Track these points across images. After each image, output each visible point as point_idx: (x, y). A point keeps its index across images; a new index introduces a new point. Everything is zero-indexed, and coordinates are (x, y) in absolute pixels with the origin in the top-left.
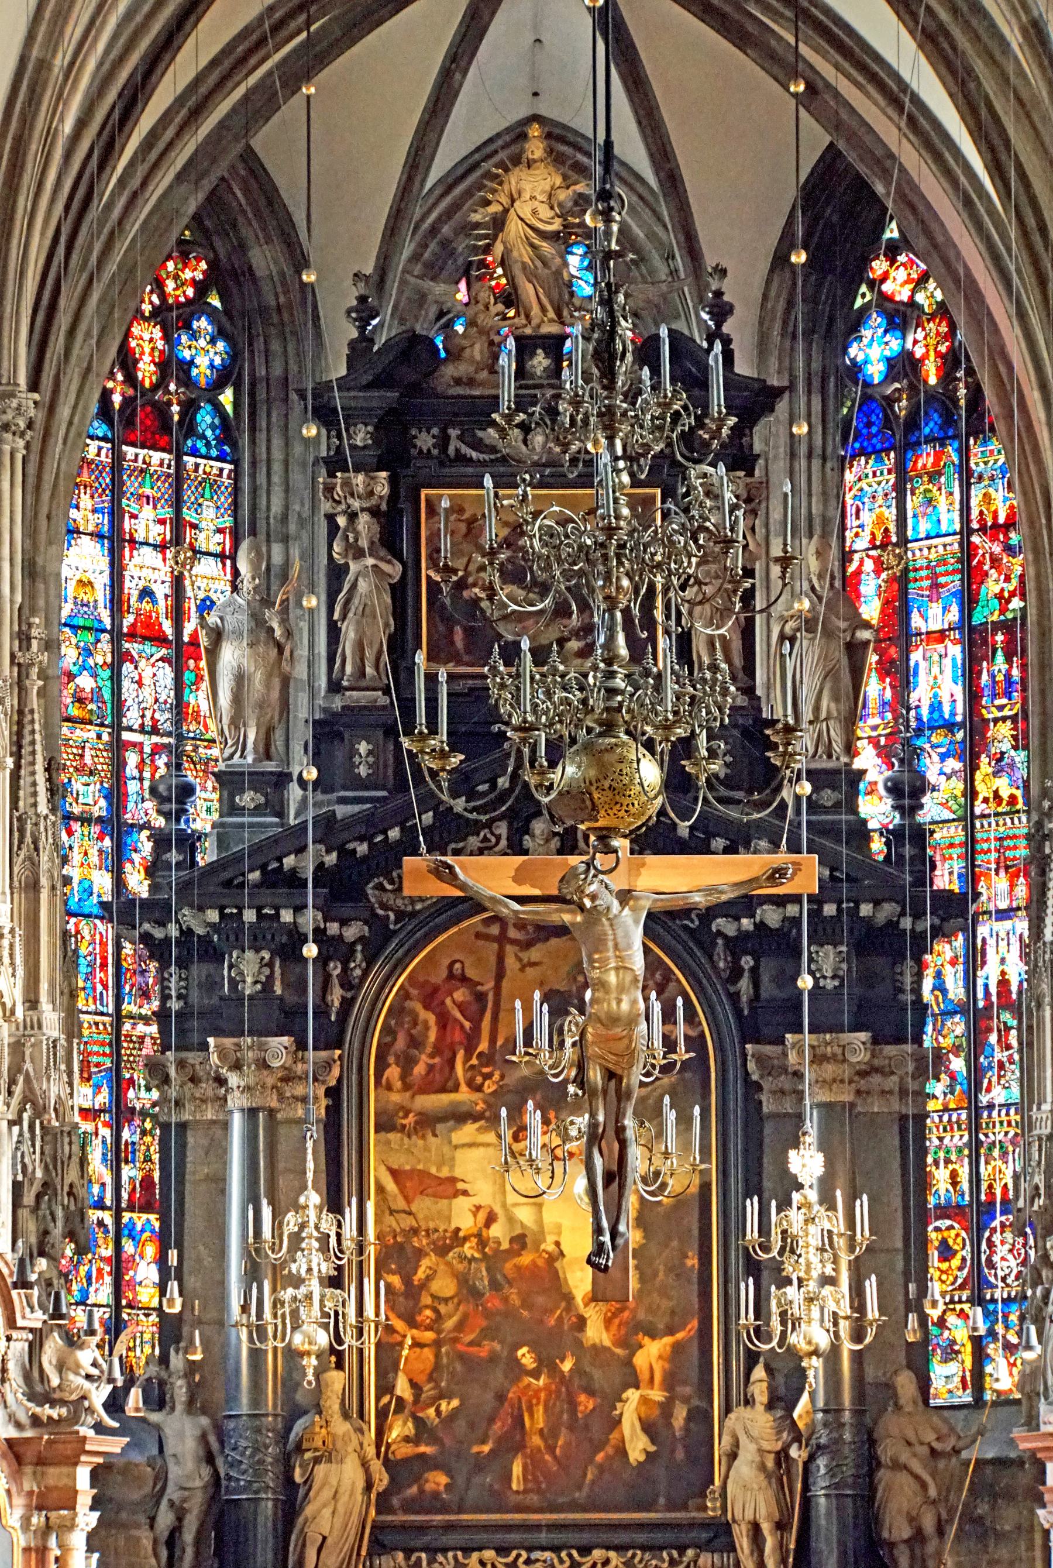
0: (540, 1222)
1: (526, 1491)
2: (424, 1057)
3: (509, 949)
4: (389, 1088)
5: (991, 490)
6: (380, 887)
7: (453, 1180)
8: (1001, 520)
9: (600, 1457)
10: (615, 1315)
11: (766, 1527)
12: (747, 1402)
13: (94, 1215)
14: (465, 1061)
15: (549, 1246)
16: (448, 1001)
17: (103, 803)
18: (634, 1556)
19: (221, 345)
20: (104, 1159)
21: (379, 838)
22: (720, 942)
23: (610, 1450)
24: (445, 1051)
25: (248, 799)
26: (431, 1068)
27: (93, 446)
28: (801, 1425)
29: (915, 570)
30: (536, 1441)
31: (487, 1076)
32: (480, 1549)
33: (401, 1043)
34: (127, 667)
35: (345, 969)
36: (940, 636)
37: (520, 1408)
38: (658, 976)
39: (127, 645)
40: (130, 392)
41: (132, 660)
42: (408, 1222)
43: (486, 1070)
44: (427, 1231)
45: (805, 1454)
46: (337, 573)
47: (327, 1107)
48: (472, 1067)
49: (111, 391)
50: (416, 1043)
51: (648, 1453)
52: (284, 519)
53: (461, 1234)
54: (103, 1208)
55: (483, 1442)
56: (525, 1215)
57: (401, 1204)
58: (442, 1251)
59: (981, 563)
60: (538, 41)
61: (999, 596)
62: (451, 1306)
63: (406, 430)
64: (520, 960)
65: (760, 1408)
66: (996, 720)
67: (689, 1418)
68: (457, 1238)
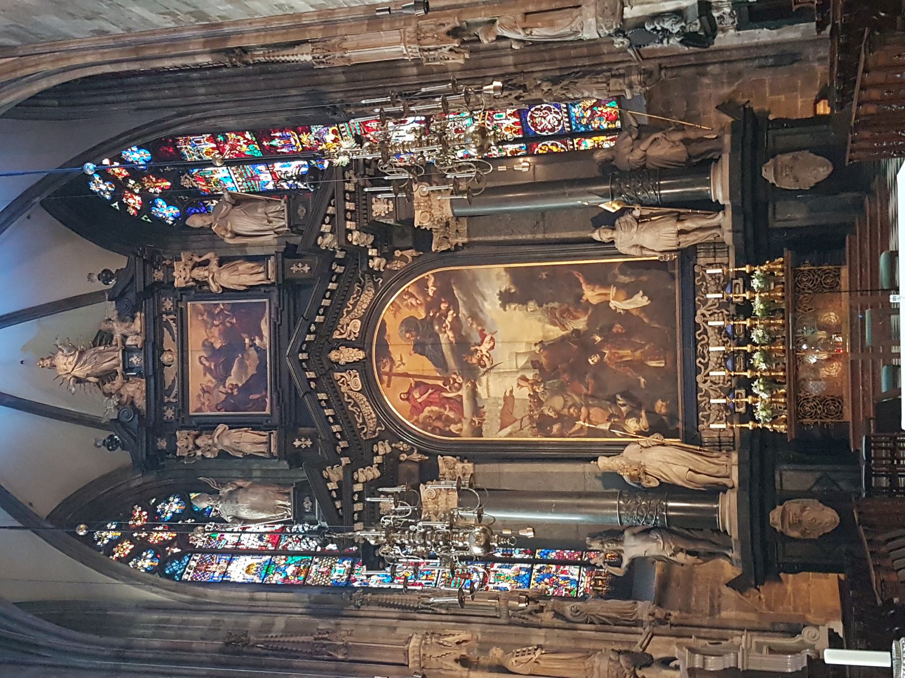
0: (525, 354)
1: (665, 359)
2: (446, 413)
3: (395, 370)
4: (461, 430)
5: (204, 152)
6: (365, 434)
7: (505, 398)
8: (214, 145)
9: (646, 320)
10: (571, 314)
11: (680, 226)
12: (613, 242)
13: (535, 574)
14: (449, 392)
15: (538, 348)
16: (419, 400)
17: (345, 562)
18: (699, 300)
19: (171, 499)
20: (508, 567)
21: (339, 436)
22: (388, 266)
23: (642, 315)
24: (444, 402)
25: (307, 505)
26: (451, 409)
27: (193, 564)
28: (618, 208)
29: (249, 188)
30: (638, 353)
31: (454, 380)
32: (697, 383)
33: (439, 424)
34: (290, 548)
35: (403, 452)
36: (272, 173)
37: (621, 362)
38: (406, 297)
39: (280, 547)
40: (176, 544)
41: (287, 545)
42: (526, 421)
43: (452, 382)
44: (531, 411)
45: (637, 207)
46: (223, 455)
47: (468, 462)
48: (450, 388)
49: (172, 553)
50: (439, 417)
51: (643, 295)
52: (243, 471)
53: (532, 393)
54: (532, 569)
55: (639, 380)
56: (522, 361)
57: (517, 424)
58: (540, 403)
59: (236, 155)
60: (22, 362)
61: (247, 144)
62: (569, 399)
63: (166, 422)
64: (399, 366)
65: (615, 235)
66: (302, 144)
67: (625, 274)
68: (534, 396)
